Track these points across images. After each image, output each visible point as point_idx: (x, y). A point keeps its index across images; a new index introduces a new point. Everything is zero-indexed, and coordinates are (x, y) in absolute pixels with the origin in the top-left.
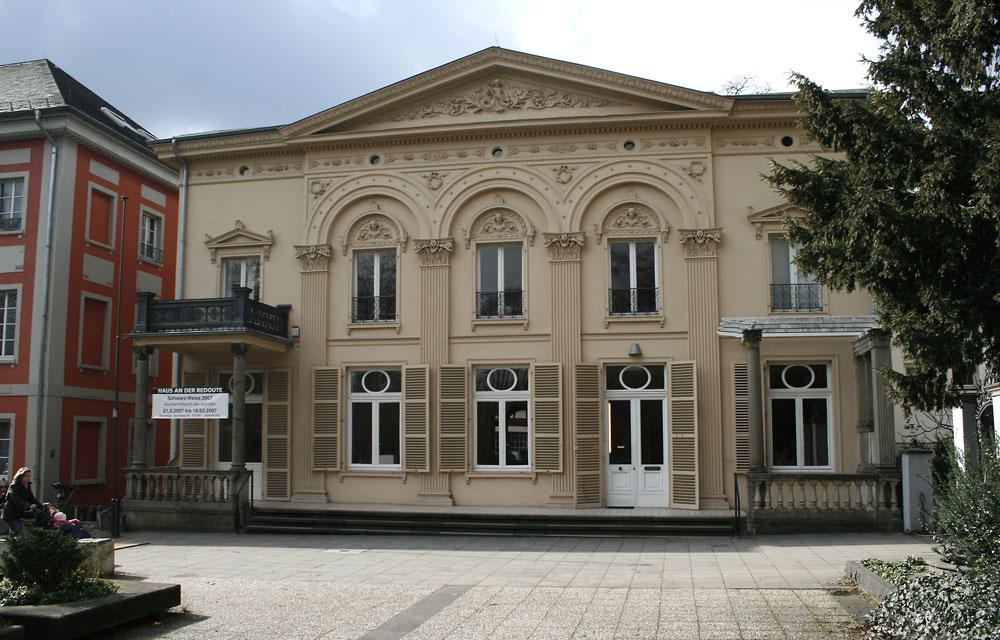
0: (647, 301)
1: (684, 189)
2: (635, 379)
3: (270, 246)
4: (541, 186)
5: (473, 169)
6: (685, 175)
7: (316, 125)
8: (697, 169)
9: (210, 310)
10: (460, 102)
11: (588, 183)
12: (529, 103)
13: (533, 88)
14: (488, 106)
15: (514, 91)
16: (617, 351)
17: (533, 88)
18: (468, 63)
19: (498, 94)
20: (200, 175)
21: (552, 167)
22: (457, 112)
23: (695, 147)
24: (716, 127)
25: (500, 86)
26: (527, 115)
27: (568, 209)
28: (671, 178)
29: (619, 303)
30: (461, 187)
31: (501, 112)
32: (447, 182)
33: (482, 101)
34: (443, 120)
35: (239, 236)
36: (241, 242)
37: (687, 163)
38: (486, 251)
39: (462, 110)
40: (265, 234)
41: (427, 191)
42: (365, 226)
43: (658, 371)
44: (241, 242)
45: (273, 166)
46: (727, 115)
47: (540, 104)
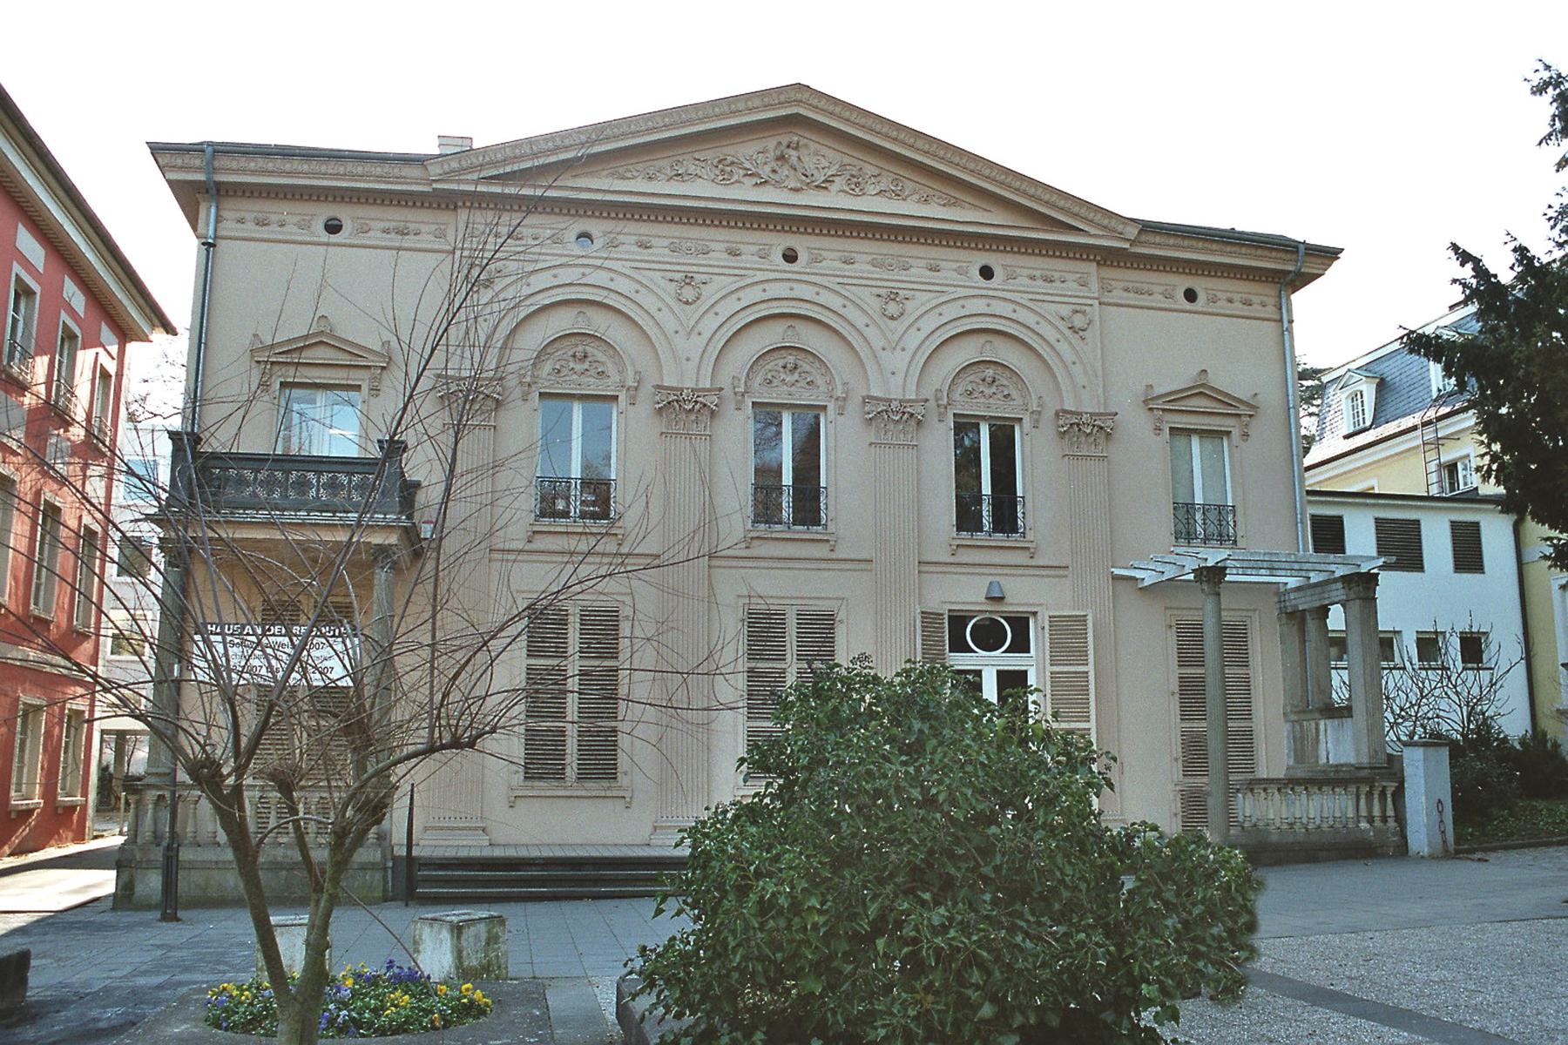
0: (1006, 518)
1: (1063, 347)
2: (989, 636)
3: (383, 368)
4: (859, 320)
5: (746, 274)
6: (1062, 326)
7: (494, 164)
8: (1079, 321)
9: (324, 478)
10: (733, 163)
11: (928, 325)
12: (839, 183)
13: (847, 160)
14: (777, 177)
15: (819, 157)
16: (966, 594)
17: (847, 160)
18: (757, 102)
19: (794, 160)
20: (241, 221)
21: (876, 291)
22: (726, 179)
23: (1076, 281)
24: (1109, 258)
25: (796, 148)
26: (835, 201)
27: (899, 361)
28: (1045, 329)
29: (967, 519)
30: (732, 305)
31: (796, 190)
32: (710, 293)
33: (767, 169)
34: (703, 189)
35: (321, 342)
36: (320, 355)
37: (1065, 310)
38: (768, 415)
39: (736, 177)
40: (377, 348)
41: (676, 307)
42: (566, 350)
43: (1020, 625)
44: (320, 355)
45: (392, 225)
46: (1127, 246)
47: (856, 185)
